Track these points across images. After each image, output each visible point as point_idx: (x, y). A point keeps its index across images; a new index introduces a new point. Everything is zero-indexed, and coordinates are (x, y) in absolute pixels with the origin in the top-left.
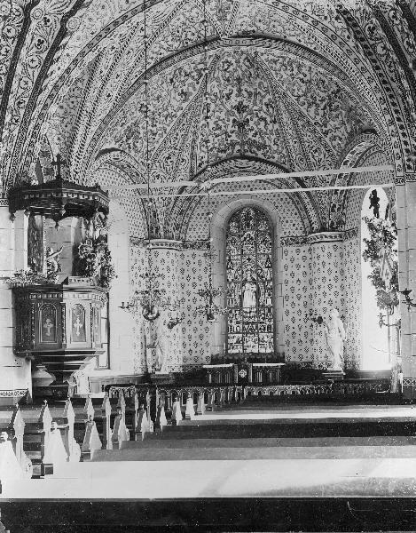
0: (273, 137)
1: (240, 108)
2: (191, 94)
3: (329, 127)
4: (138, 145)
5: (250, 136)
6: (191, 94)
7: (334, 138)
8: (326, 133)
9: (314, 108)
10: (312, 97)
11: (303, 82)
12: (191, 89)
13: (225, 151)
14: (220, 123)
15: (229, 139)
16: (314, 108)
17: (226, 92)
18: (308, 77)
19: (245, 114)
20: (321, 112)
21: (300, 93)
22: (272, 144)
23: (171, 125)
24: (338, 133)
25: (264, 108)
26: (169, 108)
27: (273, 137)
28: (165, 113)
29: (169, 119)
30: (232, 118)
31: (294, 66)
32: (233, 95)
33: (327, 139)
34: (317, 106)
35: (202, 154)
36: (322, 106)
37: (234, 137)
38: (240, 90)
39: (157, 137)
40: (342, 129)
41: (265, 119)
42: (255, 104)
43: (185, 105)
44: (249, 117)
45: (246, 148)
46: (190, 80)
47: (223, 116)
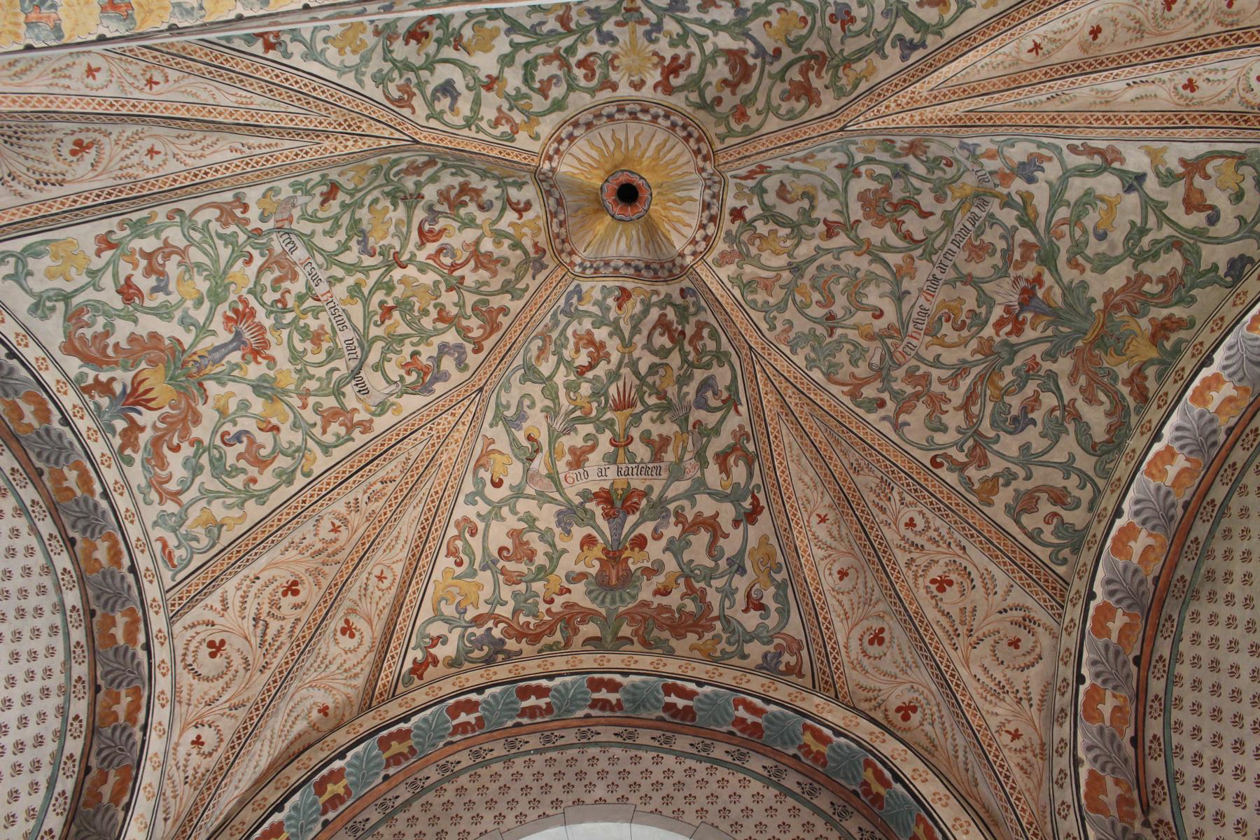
0: (741, 583)
1: (617, 503)
2: (445, 377)
3: (996, 466)
4: (176, 464)
5: (646, 594)
6: (445, 377)
7: (1024, 504)
8: (991, 485)
9: (922, 410)
10: (911, 376)
11: (870, 337)
12: (448, 364)
13: (534, 638)
14: (532, 537)
15: (560, 600)
16: (922, 410)
17: (577, 440)
18: (890, 316)
19: (632, 519)
20: (954, 419)
21: (862, 371)
22: (736, 613)
23: (338, 453)
24: (1042, 476)
25: (713, 475)
26: (349, 390)
27: (741, 583)
28: (330, 402)
29: (335, 428)
30: (579, 532)
31: (836, 289)
32: (595, 458)
33: (998, 512)
34: (937, 402)
35: (437, 629)
36: (957, 397)
37: (578, 594)
38: (621, 443)
39: (266, 479)
40: (1069, 444)
41: (711, 525)
42: (676, 473)
43: (412, 402)
44: (646, 529)
45: (626, 631)
46: (451, 337)
47: (547, 516)
